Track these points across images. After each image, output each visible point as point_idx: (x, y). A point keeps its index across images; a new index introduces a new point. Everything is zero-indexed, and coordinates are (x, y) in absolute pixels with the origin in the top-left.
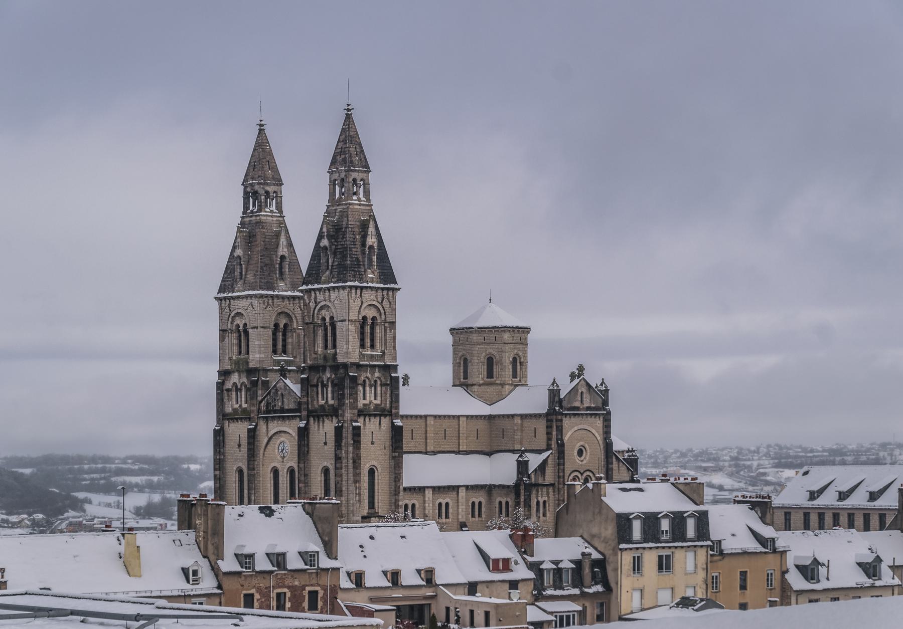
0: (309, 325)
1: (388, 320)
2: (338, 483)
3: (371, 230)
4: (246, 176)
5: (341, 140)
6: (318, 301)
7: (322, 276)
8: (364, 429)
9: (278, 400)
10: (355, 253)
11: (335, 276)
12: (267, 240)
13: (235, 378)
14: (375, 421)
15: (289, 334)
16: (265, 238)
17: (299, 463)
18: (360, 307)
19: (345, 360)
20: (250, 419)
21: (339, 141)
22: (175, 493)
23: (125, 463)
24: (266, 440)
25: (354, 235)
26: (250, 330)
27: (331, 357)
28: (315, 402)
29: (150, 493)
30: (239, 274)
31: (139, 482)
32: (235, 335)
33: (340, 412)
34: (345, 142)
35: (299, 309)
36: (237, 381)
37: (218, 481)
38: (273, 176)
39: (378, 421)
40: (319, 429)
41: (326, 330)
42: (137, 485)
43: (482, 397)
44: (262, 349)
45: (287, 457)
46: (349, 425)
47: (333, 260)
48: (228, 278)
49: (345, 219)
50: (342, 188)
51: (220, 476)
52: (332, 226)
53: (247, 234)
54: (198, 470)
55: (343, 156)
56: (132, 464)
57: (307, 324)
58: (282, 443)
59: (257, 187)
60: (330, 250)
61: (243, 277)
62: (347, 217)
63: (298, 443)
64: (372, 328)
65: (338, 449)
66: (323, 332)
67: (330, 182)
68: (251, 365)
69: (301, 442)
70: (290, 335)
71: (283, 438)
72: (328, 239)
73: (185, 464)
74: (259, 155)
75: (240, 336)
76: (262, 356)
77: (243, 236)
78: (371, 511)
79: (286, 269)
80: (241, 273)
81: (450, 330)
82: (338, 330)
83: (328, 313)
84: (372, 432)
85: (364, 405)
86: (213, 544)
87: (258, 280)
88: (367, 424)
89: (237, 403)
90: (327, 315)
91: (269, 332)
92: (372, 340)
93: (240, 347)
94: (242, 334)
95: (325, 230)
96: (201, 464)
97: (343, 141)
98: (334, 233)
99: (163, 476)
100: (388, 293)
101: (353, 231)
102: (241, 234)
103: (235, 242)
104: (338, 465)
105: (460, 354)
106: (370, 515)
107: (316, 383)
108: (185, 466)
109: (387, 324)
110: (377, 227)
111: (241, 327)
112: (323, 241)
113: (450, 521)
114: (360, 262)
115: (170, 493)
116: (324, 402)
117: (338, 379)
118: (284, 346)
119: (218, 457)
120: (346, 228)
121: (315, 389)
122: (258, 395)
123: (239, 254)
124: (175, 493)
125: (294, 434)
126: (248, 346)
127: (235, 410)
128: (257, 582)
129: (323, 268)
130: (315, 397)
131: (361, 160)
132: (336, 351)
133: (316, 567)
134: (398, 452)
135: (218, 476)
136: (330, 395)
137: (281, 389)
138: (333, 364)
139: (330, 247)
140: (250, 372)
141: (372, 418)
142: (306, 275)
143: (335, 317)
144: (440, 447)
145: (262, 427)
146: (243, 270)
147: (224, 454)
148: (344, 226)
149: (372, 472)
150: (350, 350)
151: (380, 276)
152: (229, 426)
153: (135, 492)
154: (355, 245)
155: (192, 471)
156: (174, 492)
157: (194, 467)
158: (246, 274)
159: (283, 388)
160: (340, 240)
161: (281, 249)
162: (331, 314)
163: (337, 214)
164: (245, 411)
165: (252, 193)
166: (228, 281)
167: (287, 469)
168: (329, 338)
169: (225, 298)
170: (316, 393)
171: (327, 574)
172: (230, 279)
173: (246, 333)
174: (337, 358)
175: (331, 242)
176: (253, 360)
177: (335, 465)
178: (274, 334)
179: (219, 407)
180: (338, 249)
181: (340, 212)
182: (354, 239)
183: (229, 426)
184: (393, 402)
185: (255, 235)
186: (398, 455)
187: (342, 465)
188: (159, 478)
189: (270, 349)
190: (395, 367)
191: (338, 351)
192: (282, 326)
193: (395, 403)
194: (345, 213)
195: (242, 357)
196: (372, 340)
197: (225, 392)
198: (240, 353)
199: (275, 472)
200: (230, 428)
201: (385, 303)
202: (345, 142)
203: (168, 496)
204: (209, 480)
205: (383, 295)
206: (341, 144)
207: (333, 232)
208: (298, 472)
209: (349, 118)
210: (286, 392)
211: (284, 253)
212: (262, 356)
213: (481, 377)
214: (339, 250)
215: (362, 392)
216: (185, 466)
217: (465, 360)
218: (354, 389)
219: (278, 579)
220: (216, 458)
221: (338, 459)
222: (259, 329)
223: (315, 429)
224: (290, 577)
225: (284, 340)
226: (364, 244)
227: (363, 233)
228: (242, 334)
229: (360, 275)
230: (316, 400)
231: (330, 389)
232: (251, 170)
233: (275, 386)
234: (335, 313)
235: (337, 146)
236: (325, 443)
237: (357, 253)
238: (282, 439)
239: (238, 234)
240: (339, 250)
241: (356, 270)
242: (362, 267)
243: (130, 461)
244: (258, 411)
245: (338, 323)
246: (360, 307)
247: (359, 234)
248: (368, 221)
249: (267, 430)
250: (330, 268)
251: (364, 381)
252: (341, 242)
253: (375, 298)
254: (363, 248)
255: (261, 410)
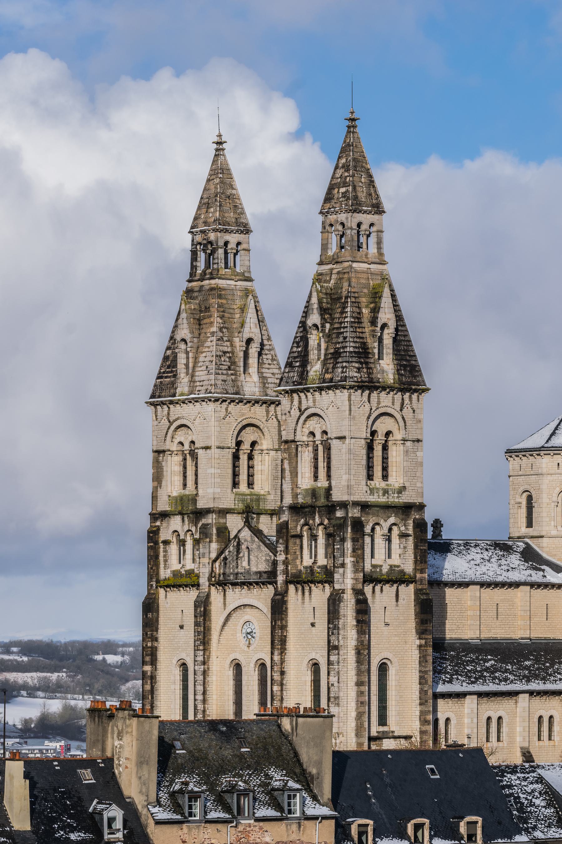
0: (290, 444)
1: (410, 438)
2: (333, 685)
3: (386, 301)
4: (196, 219)
5: (340, 165)
6: (303, 408)
7: (311, 369)
8: (373, 602)
9: (241, 557)
10: (361, 335)
11: (330, 370)
12: (226, 315)
13: (176, 523)
14: (389, 590)
15: (257, 458)
16: (224, 312)
17: (272, 653)
18: (368, 418)
19: (345, 498)
20: (197, 585)
21: (336, 168)
22: (83, 697)
23: (8, 652)
24: (222, 620)
25: (359, 308)
26: (200, 452)
27: (322, 493)
28: (298, 562)
29: (45, 698)
30: (184, 366)
31: (29, 681)
32: (178, 459)
33: (336, 576)
34: (346, 167)
35: (275, 420)
36: (179, 529)
37: (149, 682)
38: (236, 219)
39: (395, 590)
40: (303, 603)
41: (316, 450)
42: (25, 687)
43: (555, 555)
44: (218, 480)
45: (255, 645)
46: (349, 597)
47: (327, 346)
48: (168, 372)
49: (346, 285)
50: (342, 236)
51: (152, 673)
52: (326, 294)
53: (196, 307)
54: (119, 663)
55: (343, 190)
56: (18, 653)
57: (286, 442)
58: (248, 623)
59: (212, 236)
60: (322, 330)
61: (190, 371)
62: (349, 280)
63: (272, 623)
64: (385, 448)
65: (333, 633)
66: (312, 455)
67: (324, 228)
68: (201, 504)
69: (275, 623)
70: (260, 459)
71: (248, 615)
72: (321, 315)
73: (98, 654)
74: (216, 188)
75: (185, 459)
76: (218, 490)
77: (191, 309)
78: (382, 729)
79: (253, 361)
80: (187, 365)
81: (506, 453)
82: (333, 452)
83: (319, 425)
84: (385, 608)
85: (374, 566)
86: (140, 778)
87: (212, 377)
88: (376, 595)
89: (180, 563)
90: (316, 430)
91: (228, 454)
92: (385, 469)
93: (185, 477)
94: (188, 457)
95: (314, 300)
96: (123, 654)
97: (343, 167)
98: (329, 306)
99: (65, 672)
100: (410, 397)
101: (358, 302)
102: (187, 306)
103: (177, 320)
104: (333, 658)
105: (522, 489)
106: (380, 735)
107: (299, 532)
108: (99, 657)
109: (409, 442)
110: (393, 296)
111: (187, 447)
112: (311, 317)
113: (505, 745)
114: (368, 348)
115: (75, 699)
116: (313, 560)
117: (334, 526)
118: (250, 476)
119: (149, 644)
120: (347, 297)
121: (298, 541)
122: (211, 549)
123: (183, 336)
124: (83, 699)
125: (266, 609)
126: (196, 475)
127: (176, 574)
128: (206, 837)
129: (313, 355)
130: (298, 553)
131: (370, 195)
132: (330, 484)
133: (298, 814)
134: (425, 639)
135: (149, 674)
136: (321, 551)
137: (246, 540)
138: (326, 503)
139: (323, 326)
140: (199, 514)
141: (386, 587)
142: (286, 367)
143: (329, 431)
144: (490, 631)
145: (216, 596)
146: (191, 360)
147: (156, 640)
148: (344, 294)
149: (383, 668)
150: (353, 483)
151: (398, 370)
152: (166, 597)
153: (22, 696)
154: (361, 323)
155: (110, 665)
156: (81, 697)
157: (111, 659)
158: (194, 367)
159: (249, 539)
160: (337, 315)
161: (246, 329)
162: (324, 429)
163: (334, 276)
164: (190, 573)
165: (205, 245)
166: (166, 377)
167: (254, 662)
168: (321, 464)
169: (163, 403)
170: (299, 548)
171: (314, 826)
172: (169, 375)
173: (194, 455)
174: (331, 495)
175: (324, 318)
176: (204, 497)
177: (328, 658)
178: (236, 457)
179: (151, 568)
180: (334, 328)
181: (338, 273)
182: (359, 313)
183: (166, 597)
184: (418, 562)
185: (209, 308)
186: (426, 642)
187: (339, 658)
188: (59, 676)
189: (229, 481)
190: (421, 507)
191: (333, 483)
192: (246, 447)
193: (421, 563)
194: (346, 276)
195: (187, 492)
196: (385, 469)
197: (161, 546)
198: (185, 485)
199: (238, 667)
200: (168, 600)
201: (407, 412)
202: (346, 167)
203: (73, 703)
204: (137, 679)
205: (403, 399)
206: (339, 172)
207: (327, 303)
208: (272, 668)
209: (353, 132)
210: (254, 546)
211: (252, 336)
212: (218, 490)
213: (553, 524)
214: (335, 331)
215: (370, 545)
216: (99, 657)
217: (530, 498)
218: (358, 541)
219: (240, 832)
220: (146, 645)
221: (332, 648)
222: (213, 450)
223: (299, 603)
224: (257, 829)
225: (250, 467)
226: (373, 322)
227: (372, 305)
228: (188, 457)
229: (368, 368)
230: (299, 558)
231: (321, 540)
232: (204, 210)
233: (236, 536)
234: (329, 426)
235: (334, 173)
236: (313, 625)
237: (364, 335)
238: (247, 618)
239: (183, 307)
240: (335, 331)
241: (363, 361)
242: (370, 356)
243: (15, 649)
244: (211, 574)
245: (334, 441)
246: (368, 418)
247: (367, 307)
248: (381, 286)
249: (225, 604)
250: (322, 357)
251: (373, 529)
252: (339, 318)
253: (390, 404)
254: (373, 328)
255: (215, 573)
